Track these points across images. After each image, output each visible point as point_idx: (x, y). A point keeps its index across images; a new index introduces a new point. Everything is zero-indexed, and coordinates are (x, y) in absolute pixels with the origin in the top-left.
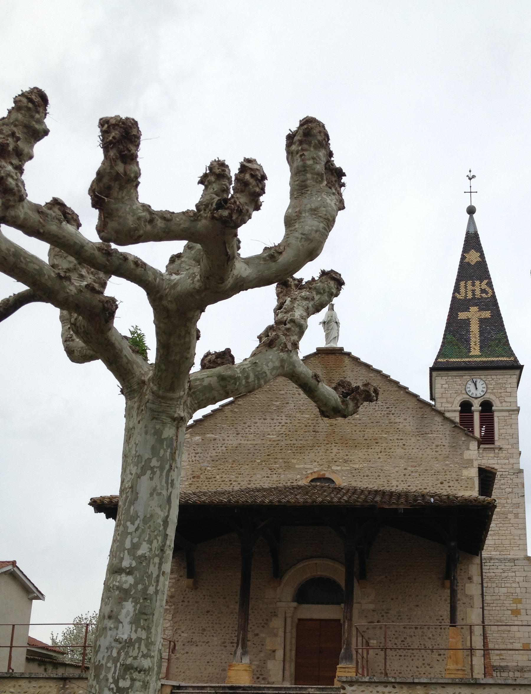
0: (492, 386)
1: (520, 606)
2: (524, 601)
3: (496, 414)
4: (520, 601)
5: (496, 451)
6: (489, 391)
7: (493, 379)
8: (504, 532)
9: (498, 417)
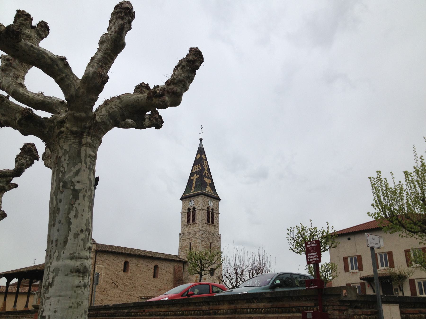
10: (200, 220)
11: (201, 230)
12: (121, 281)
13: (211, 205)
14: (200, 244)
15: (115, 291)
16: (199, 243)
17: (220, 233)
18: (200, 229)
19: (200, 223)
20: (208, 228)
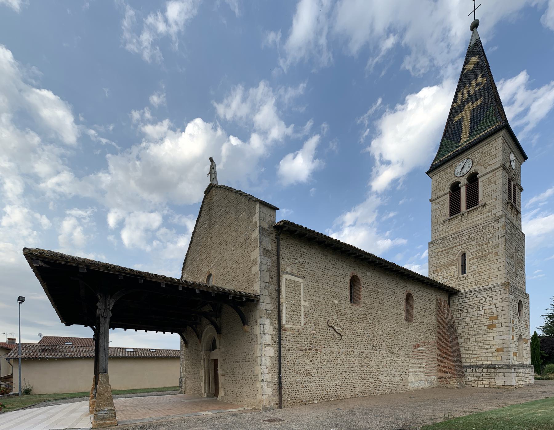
1: (495, 321)
2: (499, 317)
4: (496, 318)
8: (484, 269)
12: (347, 324)
15: (335, 349)
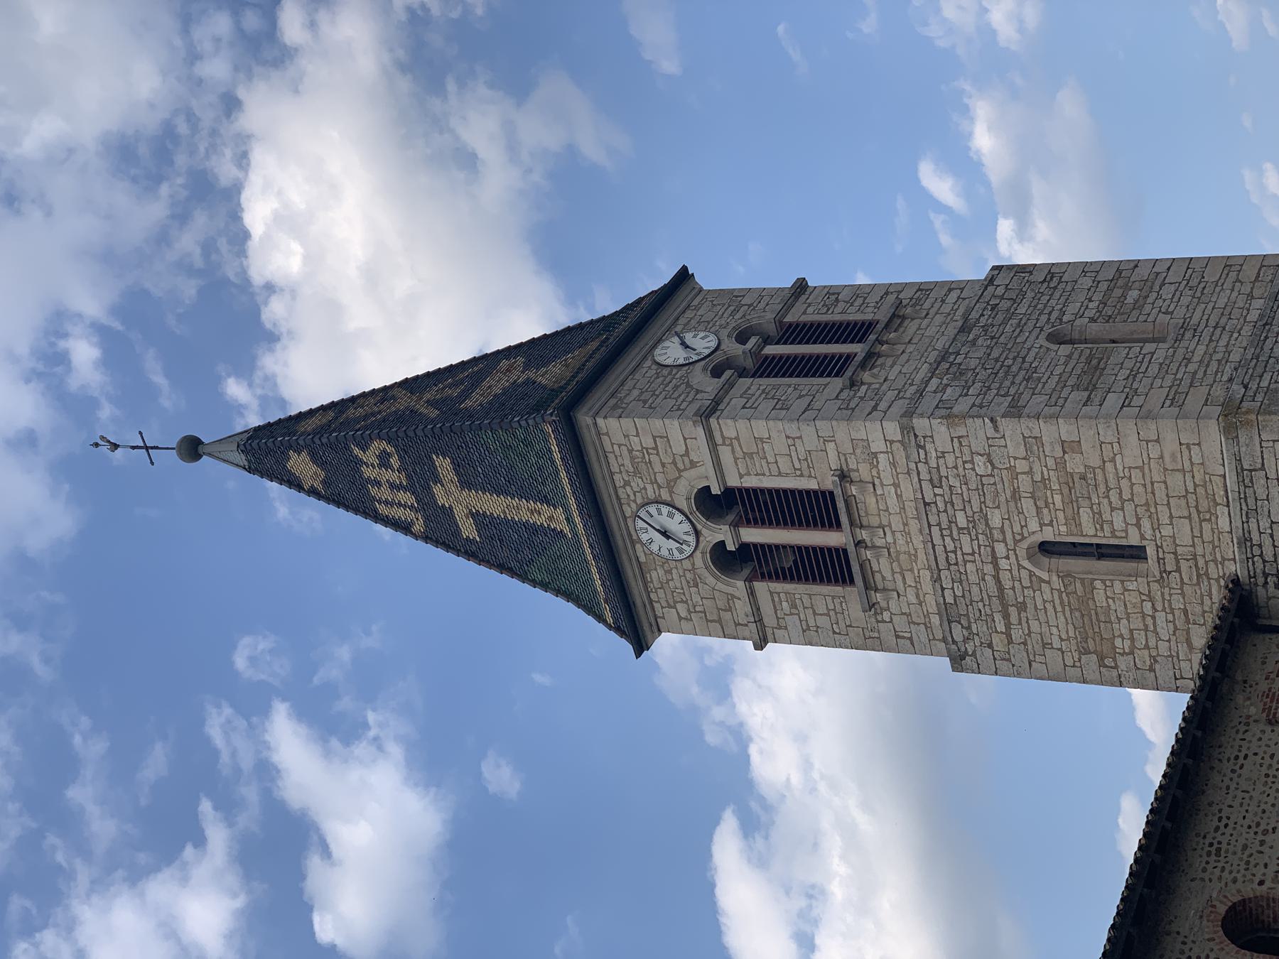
0: (649, 487)
3: (733, 482)
5: (854, 490)
6: (665, 496)
7: (627, 483)
9: (741, 476)
10: (808, 431)
11: (907, 430)
13: (703, 343)
14: (1047, 431)
16: (1032, 444)
17: (982, 274)
18: (893, 429)
19: (843, 432)
20: (904, 366)
